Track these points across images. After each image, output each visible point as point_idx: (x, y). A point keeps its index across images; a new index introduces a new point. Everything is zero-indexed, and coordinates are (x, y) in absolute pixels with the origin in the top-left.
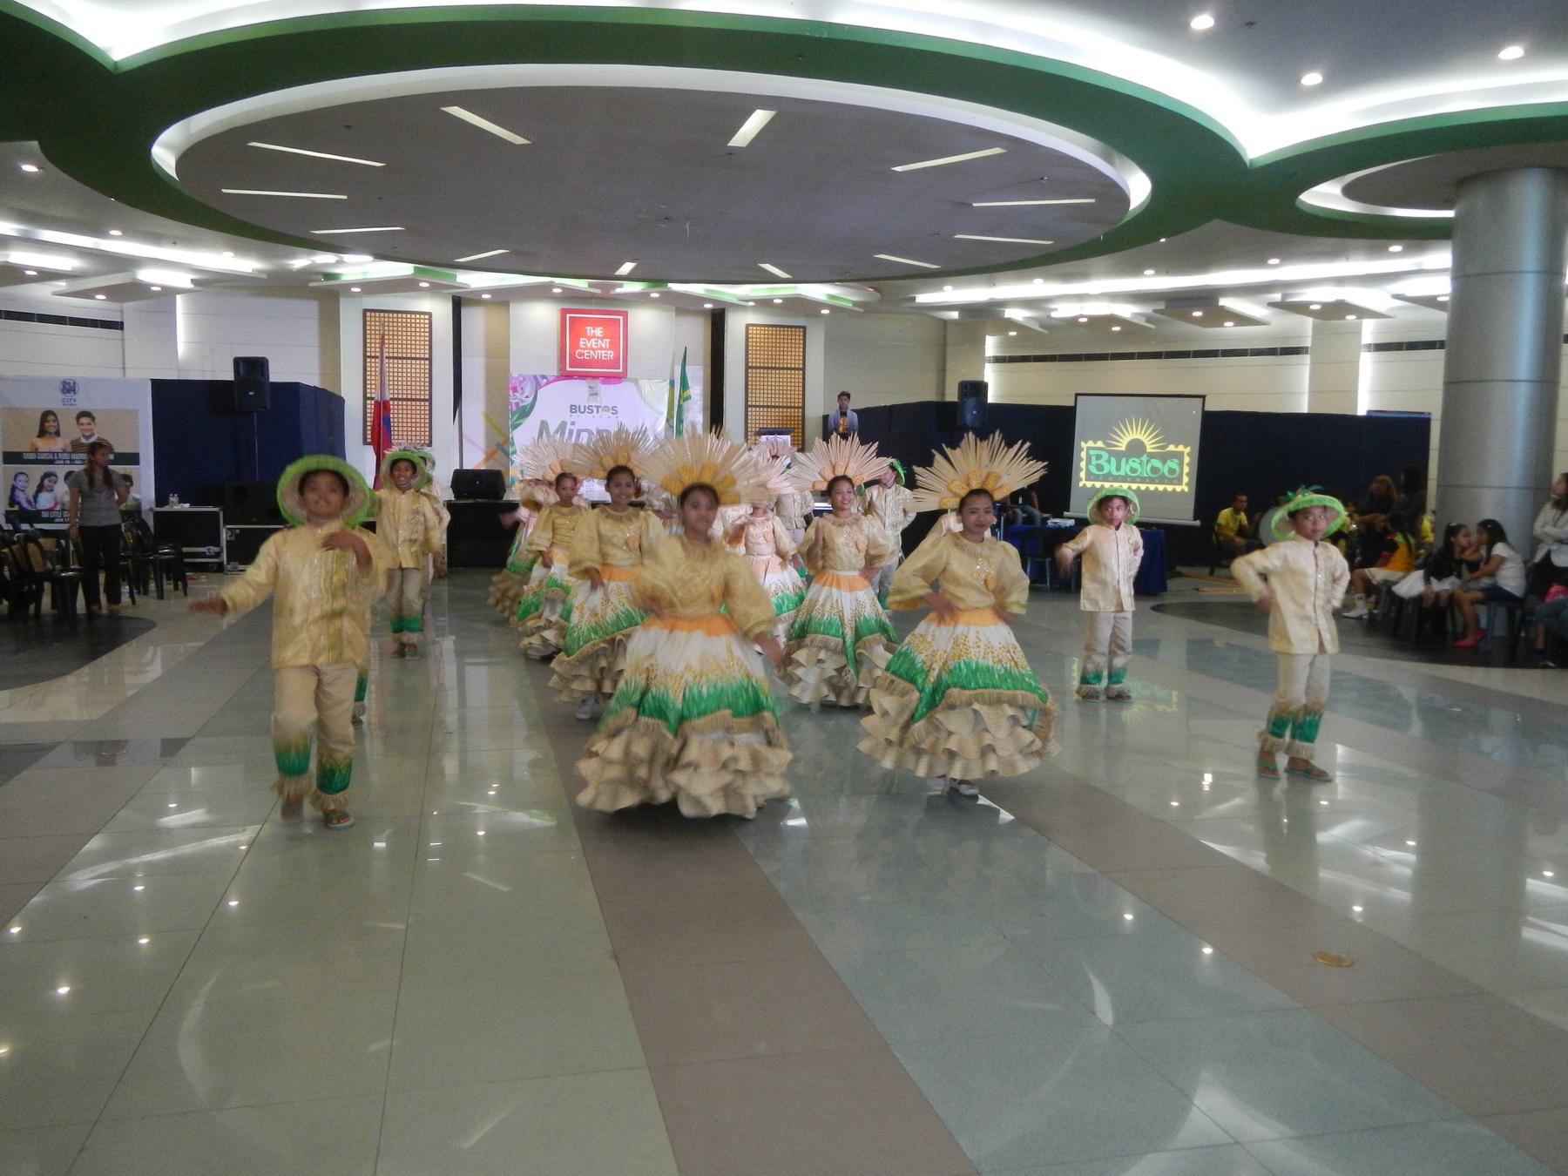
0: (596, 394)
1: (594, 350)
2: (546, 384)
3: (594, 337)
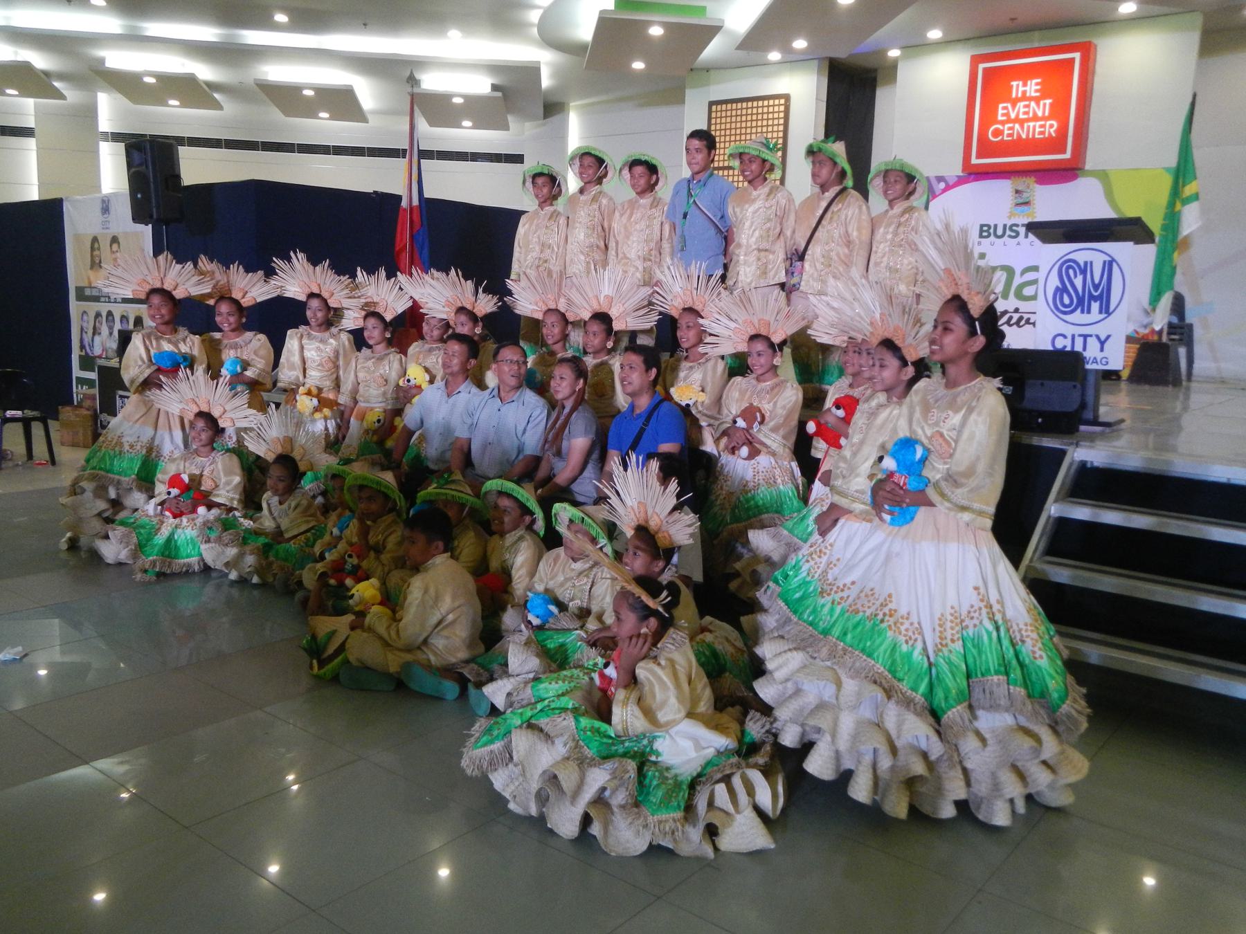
0: (1027, 203)
1: (1022, 122)
2: (944, 191)
3: (1024, 97)
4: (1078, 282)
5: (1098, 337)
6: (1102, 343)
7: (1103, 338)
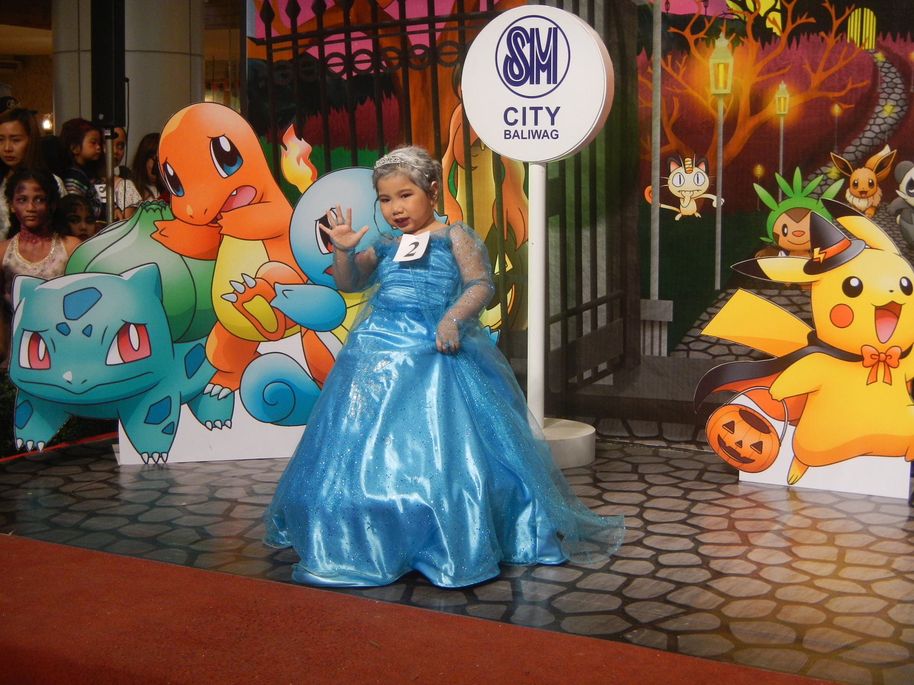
4: (526, 50)
5: (548, 109)
6: (553, 116)
7: (553, 112)
